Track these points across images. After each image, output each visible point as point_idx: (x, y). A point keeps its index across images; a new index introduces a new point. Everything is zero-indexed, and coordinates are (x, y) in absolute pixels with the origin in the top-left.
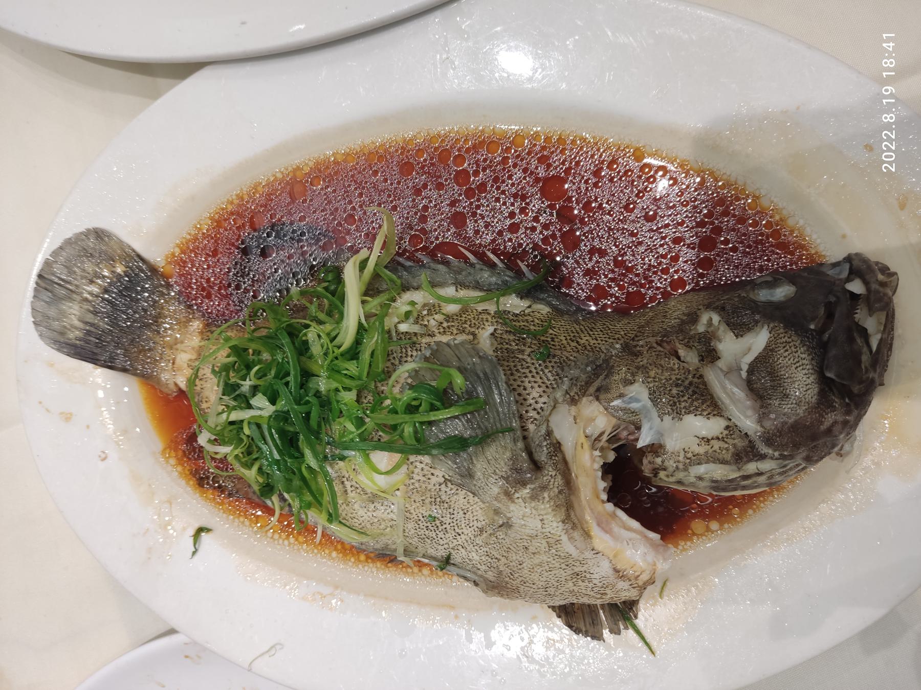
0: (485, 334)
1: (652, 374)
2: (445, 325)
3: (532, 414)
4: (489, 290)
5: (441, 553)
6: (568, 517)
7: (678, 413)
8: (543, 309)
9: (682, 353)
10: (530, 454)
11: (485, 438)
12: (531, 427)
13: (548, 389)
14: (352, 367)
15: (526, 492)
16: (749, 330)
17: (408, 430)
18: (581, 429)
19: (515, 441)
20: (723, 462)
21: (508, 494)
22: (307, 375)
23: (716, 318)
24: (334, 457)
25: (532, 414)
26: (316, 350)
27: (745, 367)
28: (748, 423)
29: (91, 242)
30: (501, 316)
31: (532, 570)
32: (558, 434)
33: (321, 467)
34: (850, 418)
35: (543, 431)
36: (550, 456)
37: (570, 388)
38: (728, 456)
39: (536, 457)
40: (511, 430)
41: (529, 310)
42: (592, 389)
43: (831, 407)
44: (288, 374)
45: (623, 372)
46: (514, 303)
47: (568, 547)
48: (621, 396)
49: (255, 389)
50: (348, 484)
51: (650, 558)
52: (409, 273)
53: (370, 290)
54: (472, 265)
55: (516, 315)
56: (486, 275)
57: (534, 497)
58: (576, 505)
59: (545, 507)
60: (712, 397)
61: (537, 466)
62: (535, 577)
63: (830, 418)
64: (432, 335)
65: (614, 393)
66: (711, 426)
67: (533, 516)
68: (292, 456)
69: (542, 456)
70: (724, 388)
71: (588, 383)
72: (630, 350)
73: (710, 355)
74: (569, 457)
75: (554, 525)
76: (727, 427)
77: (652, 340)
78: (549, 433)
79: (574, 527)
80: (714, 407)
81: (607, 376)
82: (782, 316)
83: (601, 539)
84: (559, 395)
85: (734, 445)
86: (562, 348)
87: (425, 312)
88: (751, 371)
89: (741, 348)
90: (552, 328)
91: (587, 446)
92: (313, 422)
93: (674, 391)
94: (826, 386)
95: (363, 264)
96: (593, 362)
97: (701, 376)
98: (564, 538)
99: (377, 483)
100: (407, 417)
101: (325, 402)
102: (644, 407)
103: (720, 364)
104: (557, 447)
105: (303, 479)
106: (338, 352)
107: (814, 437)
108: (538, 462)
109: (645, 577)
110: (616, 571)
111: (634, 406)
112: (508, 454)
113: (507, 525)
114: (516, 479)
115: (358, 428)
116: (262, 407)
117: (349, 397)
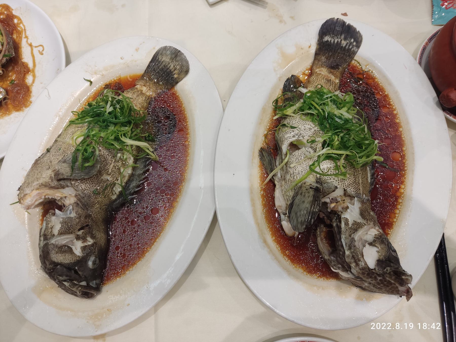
0: (109, 178)
1: (77, 220)
2: (117, 167)
3: (77, 184)
10: (64, 179)
11: (72, 169)
12: (73, 183)
15: (53, 176)
17: (80, 148)
18: (68, 196)
19: (67, 176)
25: (77, 184)
28: (53, 241)
29: (185, 69)
30: (115, 184)
32: (67, 188)
35: (69, 184)
36: (61, 185)
37: (80, 196)
39: (62, 181)
40: (71, 176)
41: (114, 193)
42: (79, 202)
45: (80, 211)
46: (118, 189)
47: (36, 183)
48: (73, 209)
54: (140, 181)
55: (112, 188)
57: (51, 177)
58: (46, 188)
59: (47, 180)
60: (65, 234)
61: (59, 180)
65: (75, 208)
66: (56, 232)
67: (46, 175)
69: (62, 182)
70: (67, 238)
71: (81, 202)
72: (88, 216)
74: (60, 190)
75: (41, 181)
76: (54, 235)
78: (68, 186)
79: (40, 186)
80: (61, 233)
81: (81, 208)
83: (35, 192)
84: (80, 193)
85: (48, 235)
86: (96, 198)
87: (124, 163)
88: (68, 247)
89: (78, 248)
90: (105, 197)
95: (148, 149)
97: (72, 233)
100: (84, 148)
102: (67, 214)
103: (75, 240)
104: (63, 188)
108: (60, 180)
111: (69, 212)
114: (57, 174)
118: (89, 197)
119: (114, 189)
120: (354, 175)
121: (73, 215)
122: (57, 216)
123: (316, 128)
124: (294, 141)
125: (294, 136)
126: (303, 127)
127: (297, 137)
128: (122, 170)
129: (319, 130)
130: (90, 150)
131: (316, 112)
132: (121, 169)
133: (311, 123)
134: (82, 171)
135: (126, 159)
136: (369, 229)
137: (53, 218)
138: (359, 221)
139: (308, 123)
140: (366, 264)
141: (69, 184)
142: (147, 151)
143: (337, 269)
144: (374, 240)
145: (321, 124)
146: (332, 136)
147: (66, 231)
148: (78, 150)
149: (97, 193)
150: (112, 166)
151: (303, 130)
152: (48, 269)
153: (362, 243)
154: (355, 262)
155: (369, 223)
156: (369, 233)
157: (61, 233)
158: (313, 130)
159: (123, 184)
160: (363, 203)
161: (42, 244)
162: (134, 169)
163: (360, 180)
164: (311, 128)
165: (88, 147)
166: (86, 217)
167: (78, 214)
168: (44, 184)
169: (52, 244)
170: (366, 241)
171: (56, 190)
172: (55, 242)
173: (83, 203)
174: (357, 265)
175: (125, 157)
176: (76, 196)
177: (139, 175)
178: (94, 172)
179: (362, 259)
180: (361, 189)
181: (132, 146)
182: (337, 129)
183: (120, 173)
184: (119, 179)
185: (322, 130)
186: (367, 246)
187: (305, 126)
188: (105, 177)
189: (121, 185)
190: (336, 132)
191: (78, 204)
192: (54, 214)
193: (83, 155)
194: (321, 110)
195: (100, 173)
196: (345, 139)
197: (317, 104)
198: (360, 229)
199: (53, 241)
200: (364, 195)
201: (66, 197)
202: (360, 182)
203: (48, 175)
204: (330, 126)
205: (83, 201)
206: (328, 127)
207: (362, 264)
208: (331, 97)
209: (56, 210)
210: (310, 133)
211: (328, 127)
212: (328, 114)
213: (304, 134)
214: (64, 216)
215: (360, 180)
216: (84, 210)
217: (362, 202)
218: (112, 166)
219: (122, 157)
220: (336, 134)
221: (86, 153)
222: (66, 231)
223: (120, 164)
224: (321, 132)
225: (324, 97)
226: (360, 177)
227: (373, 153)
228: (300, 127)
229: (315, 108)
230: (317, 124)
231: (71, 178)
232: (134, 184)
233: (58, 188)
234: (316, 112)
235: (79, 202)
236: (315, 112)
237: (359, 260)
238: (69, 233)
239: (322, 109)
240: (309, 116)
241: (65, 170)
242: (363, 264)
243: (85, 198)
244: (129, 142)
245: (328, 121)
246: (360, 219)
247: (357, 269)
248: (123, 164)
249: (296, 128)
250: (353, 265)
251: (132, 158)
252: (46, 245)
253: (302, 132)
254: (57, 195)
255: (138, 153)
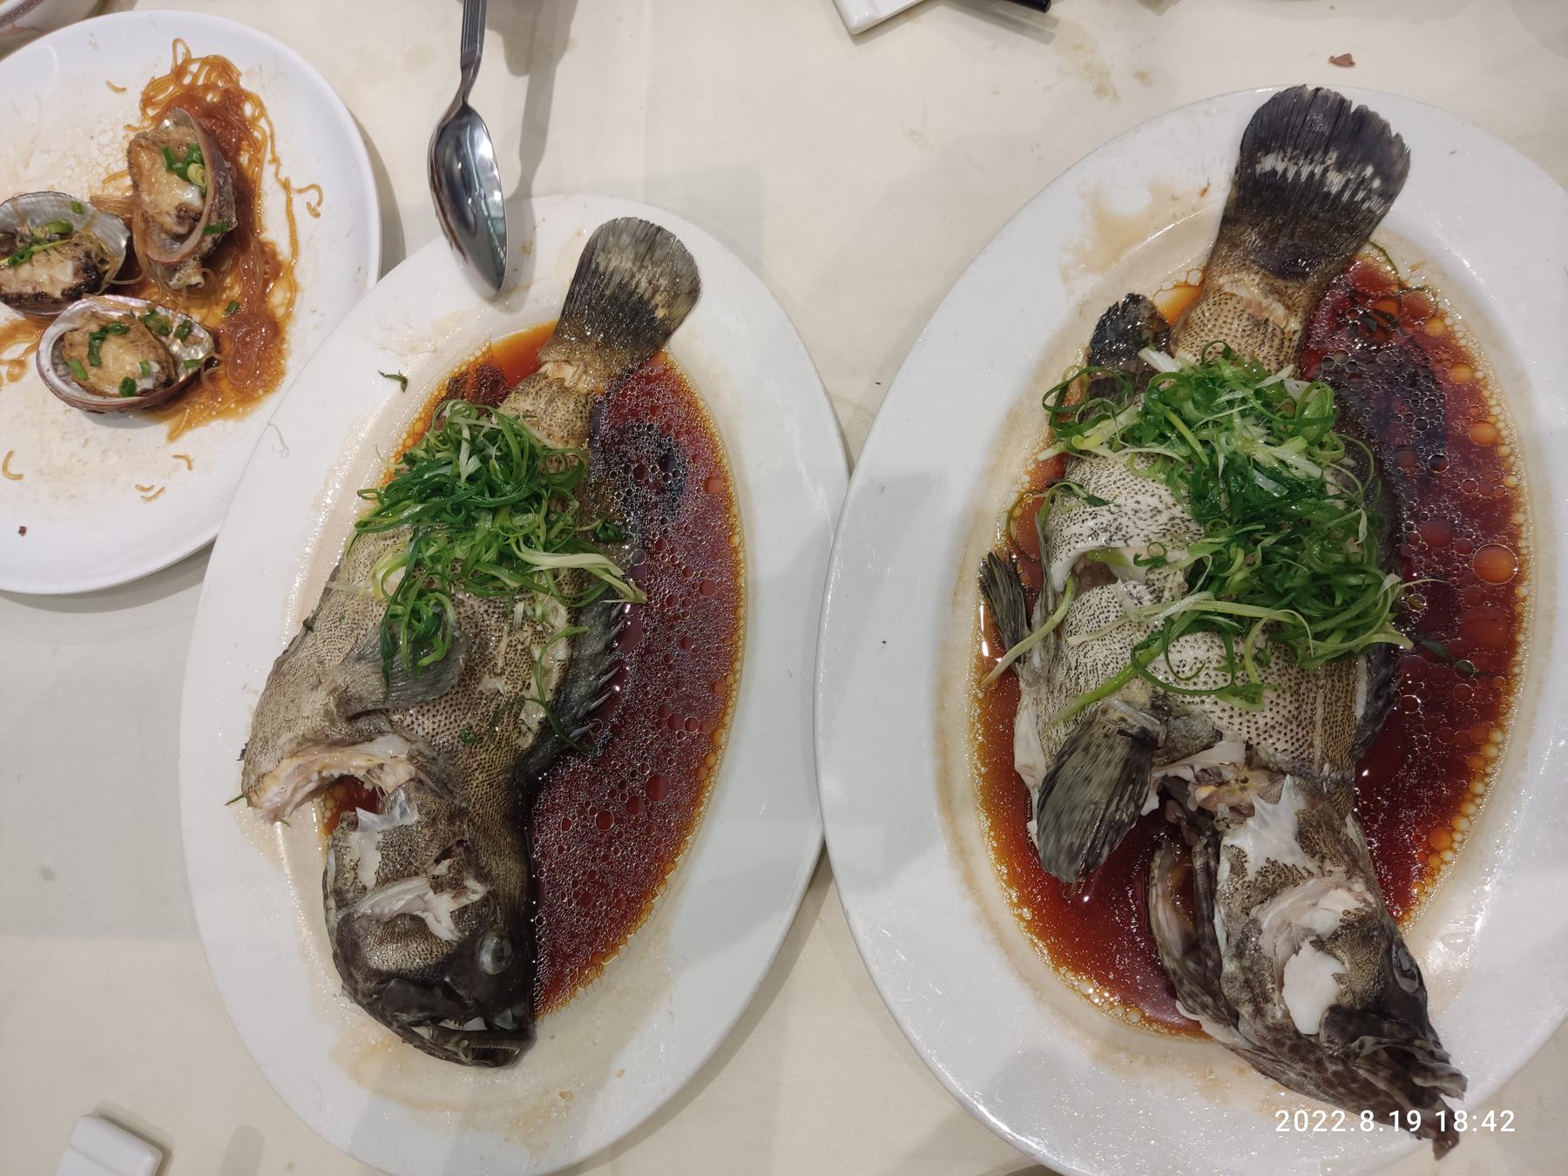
0: (500, 684)
1: (425, 831)
2: (520, 647)
3: (409, 720)
4: (558, 691)
5: (318, 624)
6: (308, 740)
7: (384, 848)
8: (527, 742)
9: (446, 863)
10: (368, 713)
11: (388, 676)
12: (396, 718)
13: (429, 740)
14: (492, 555)
15: (332, 706)
16: (457, 924)
17: (399, 609)
18: (387, 760)
20: (336, 880)
21: (335, 690)
22: (494, 511)
23: (476, 897)
24: (416, 531)
26: (519, 520)
27: (423, 915)
28: (365, 907)
30: (521, 701)
31: (277, 703)
32: (380, 739)
33: (406, 520)
34: (360, 996)
36: (360, 731)
38: (340, 884)
40: (386, 699)
41: (524, 728)
42: (422, 776)
43: (366, 980)
44: (492, 496)
46: (534, 715)
47: (285, 737)
48: (409, 800)
49: (485, 460)
50: (390, 542)
51: (268, 804)
52: (601, 614)
53: (581, 576)
54: (599, 677)
55: (517, 716)
56: (583, 691)
57: (327, 713)
59: (318, 722)
62: (271, 706)
63: (359, 977)
64: (509, 633)
66: (368, 877)
67: (314, 706)
68: (420, 492)
69: (362, 724)
71: (428, 773)
72: (456, 815)
73: (438, 885)
75: (301, 729)
76: (365, 888)
77: (467, 836)
78: (381, 733)
80: (387, 879)
82: (460, 956)
83: (289, 765)
84: (421, 746)
86: (472, 755)
87: (539, 628)
89: (441, 915)
91: (370, 764)
92: (444, 516)
93: (406, 848)
94: (384, 977)
96: (450, 781)
97: (417, 874)
98: (291, 735)
99: (385, 568)
101: (469, 524)
105: (400, 501)
106: (512, 542)
107: (346, 960)
108: (356, 718)
109: (254, 798)
110: (263, 775)
111: (397, 811)
112: (365, 694)
113: (315, 688)
115: (431, 557)
116: (468, 465)
117: (460, 551)
118: (452, 753)
119: (523, 716)
120: (1297, 692)
121: (413, 817)
122: (365, 830)
123: (1177, 512)
124: (1093, 552)
125: (1094, 534)
126: (1131, 502)
127: (1103, 538)
128: (537, 653)
129: (1186, 516)
130: (428, 612)
131: (1184, 451)
132: (533, 652)
133: (1163, 491)
134: (417, 681)
135: (544, 616)
136: (1326, 890)
137: (355, 837)
138: (1289, 861)
139: (1151, 486)
140: (1287, 1014)
141: (385, 727)
142: (607, 577)
143: (1198, 1009)
144: (1335, 933)
145: (1197, 496)
146: (1227, 546)
147: (398, 869)
148: (394, 616)
149: (472, 739)
150: (503, 645)
151: (1131, 513)
152: (364, 995)
153: (1290, 939)
154: (1253, 1001)
155: (1328, 866)
156: (1324, 903)
157: (384, 881)
158: (1163, 518)
159: (548, 697)
160: (1314, 797)
161: (336, 917)
162: (574, 641)
163: (1320, 710)
164: (1161, 507)
165: (422, 604)
166: (451, 819)
167: (428, 813)
168: (309, 736)
169: (364, 915)
170: (1308, 931)
171: (350, 750)
172: (372, 907)
173: (436, 776)
174: (1259, 1012)
175: (539, 612)
176: (411, 758)
177: (594, 659)
178: (452, 676)
179: (1276, 997)
180: (1317, 742)
181: (555, 573)
182: (1252, 520)
183: (532, 664)
184: (533, 681)
185: (1200, 518)
186: (1307, 949)
187: (1139, 497)
188: (489, 684)
189: (541, 702)
190: (1250, 533)
191: (421, 781)
192: (354, 824)
193: (409, 626)
194: (1199, 449)
195: (471, 674)
196: (1280, 561)
197: (1189, 424)
198: (1286, 891)
199: (365, 907)
200: (1326, 767)
201: (381, 766)
202: (1318, 718)
203: (318, 706)
204: (1230, 505)
205: (435, 769)
206: (1224, 507)
207: (1275, 1013)
208: (1244, 400)
209: (360, 811)
210: (1153, 527)
211: (1224, 507)
212: (1230, 461)
213: (1132, 531)
214: (386, 827)
215: (1320, 710)
216: (441, 797)
217: (1313, 792)
218: (503, 645)
219: (530, 613)
220: (1249, 541)
221: (419, 621)
222: (398, 869)
223: (526, 634)
224: (1193, 526)
225: (1219, 400)
226: (1320, 700)
227: (1379, 618)
228: (1120, 501)
229: (1181, 438)
230: (1184, 493)
231: (387, 706)
232: (580, 690)
233: (354, 743)
234: (1184, 451)
235: (422, 776)
236: (1177, 452)
237: (1267, 1000)
238: (410, 876)
239: (1205, 443)
240: (1159, 465)
241: (367, 683)
242: (1279, 1014)
243: (441, 761)
244: (546, 561)
245: (1227, 482)
246: (1293, 852)
247: (1259, 1025)
248: (536, 632)
249: (1105, 503)
250: (1246, 1010)
251: (563, 611)
252: (346, 922)
253: (1124, 521)
254: (354, 762)
255: (581, 589)
